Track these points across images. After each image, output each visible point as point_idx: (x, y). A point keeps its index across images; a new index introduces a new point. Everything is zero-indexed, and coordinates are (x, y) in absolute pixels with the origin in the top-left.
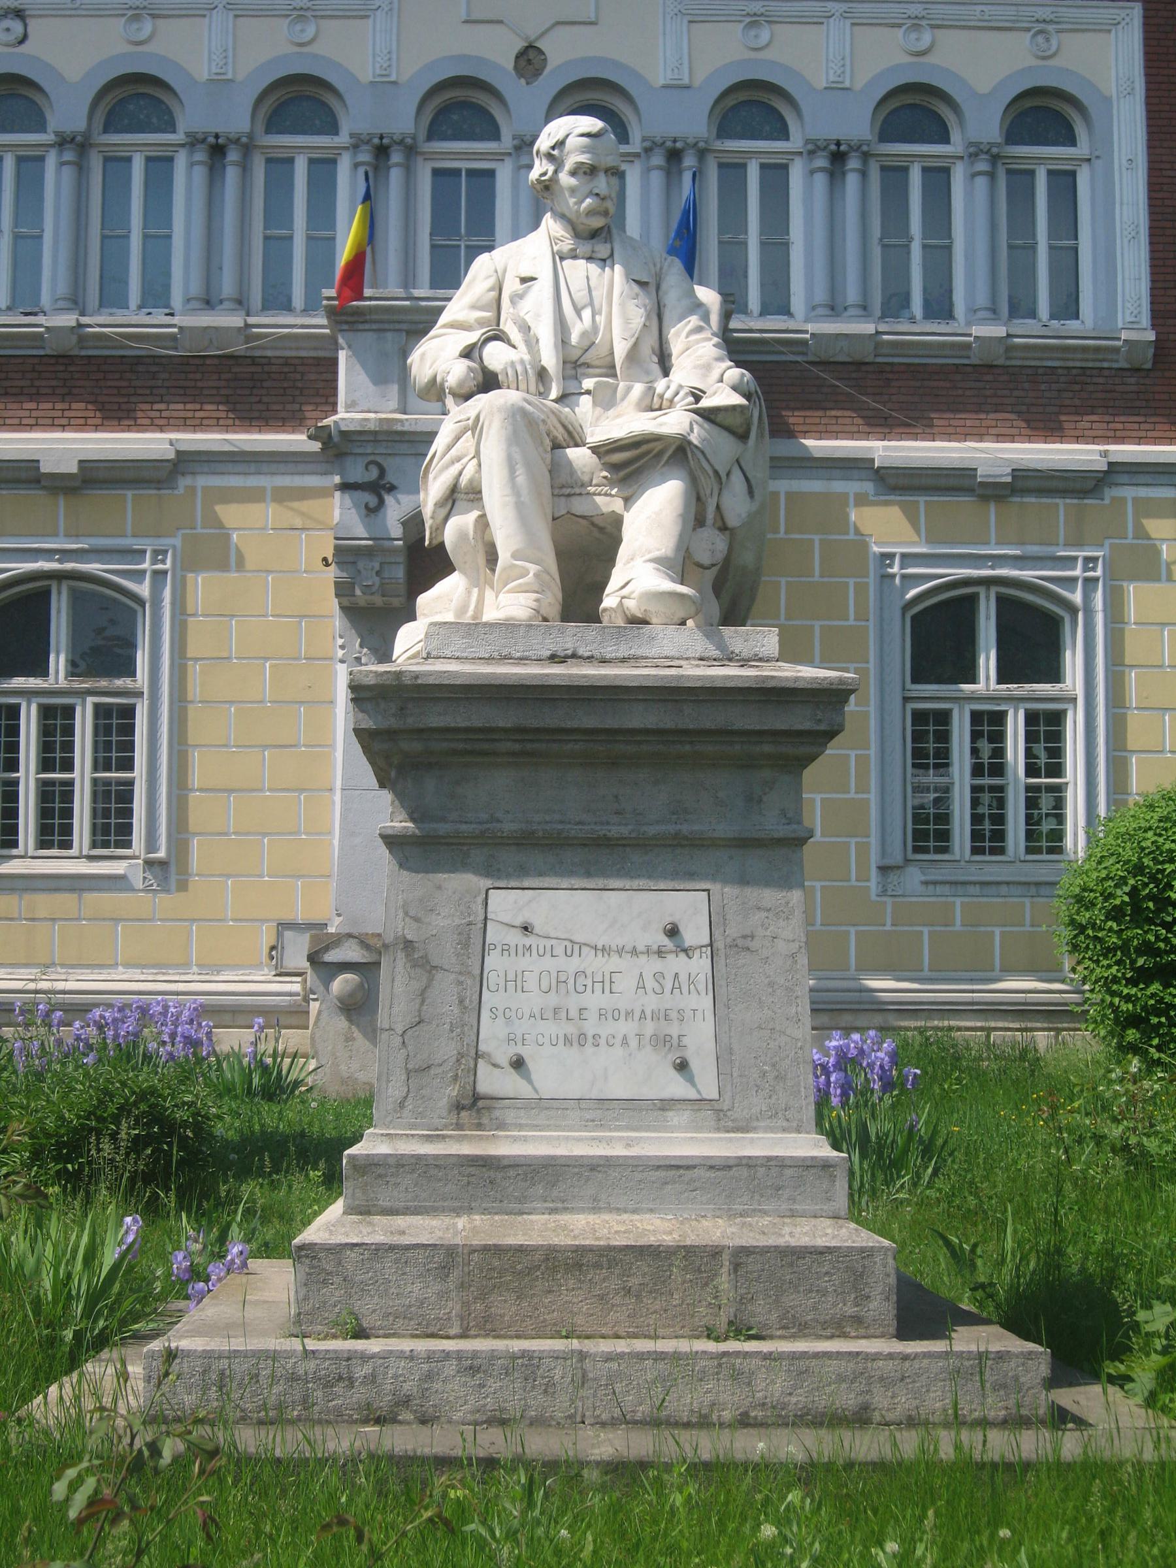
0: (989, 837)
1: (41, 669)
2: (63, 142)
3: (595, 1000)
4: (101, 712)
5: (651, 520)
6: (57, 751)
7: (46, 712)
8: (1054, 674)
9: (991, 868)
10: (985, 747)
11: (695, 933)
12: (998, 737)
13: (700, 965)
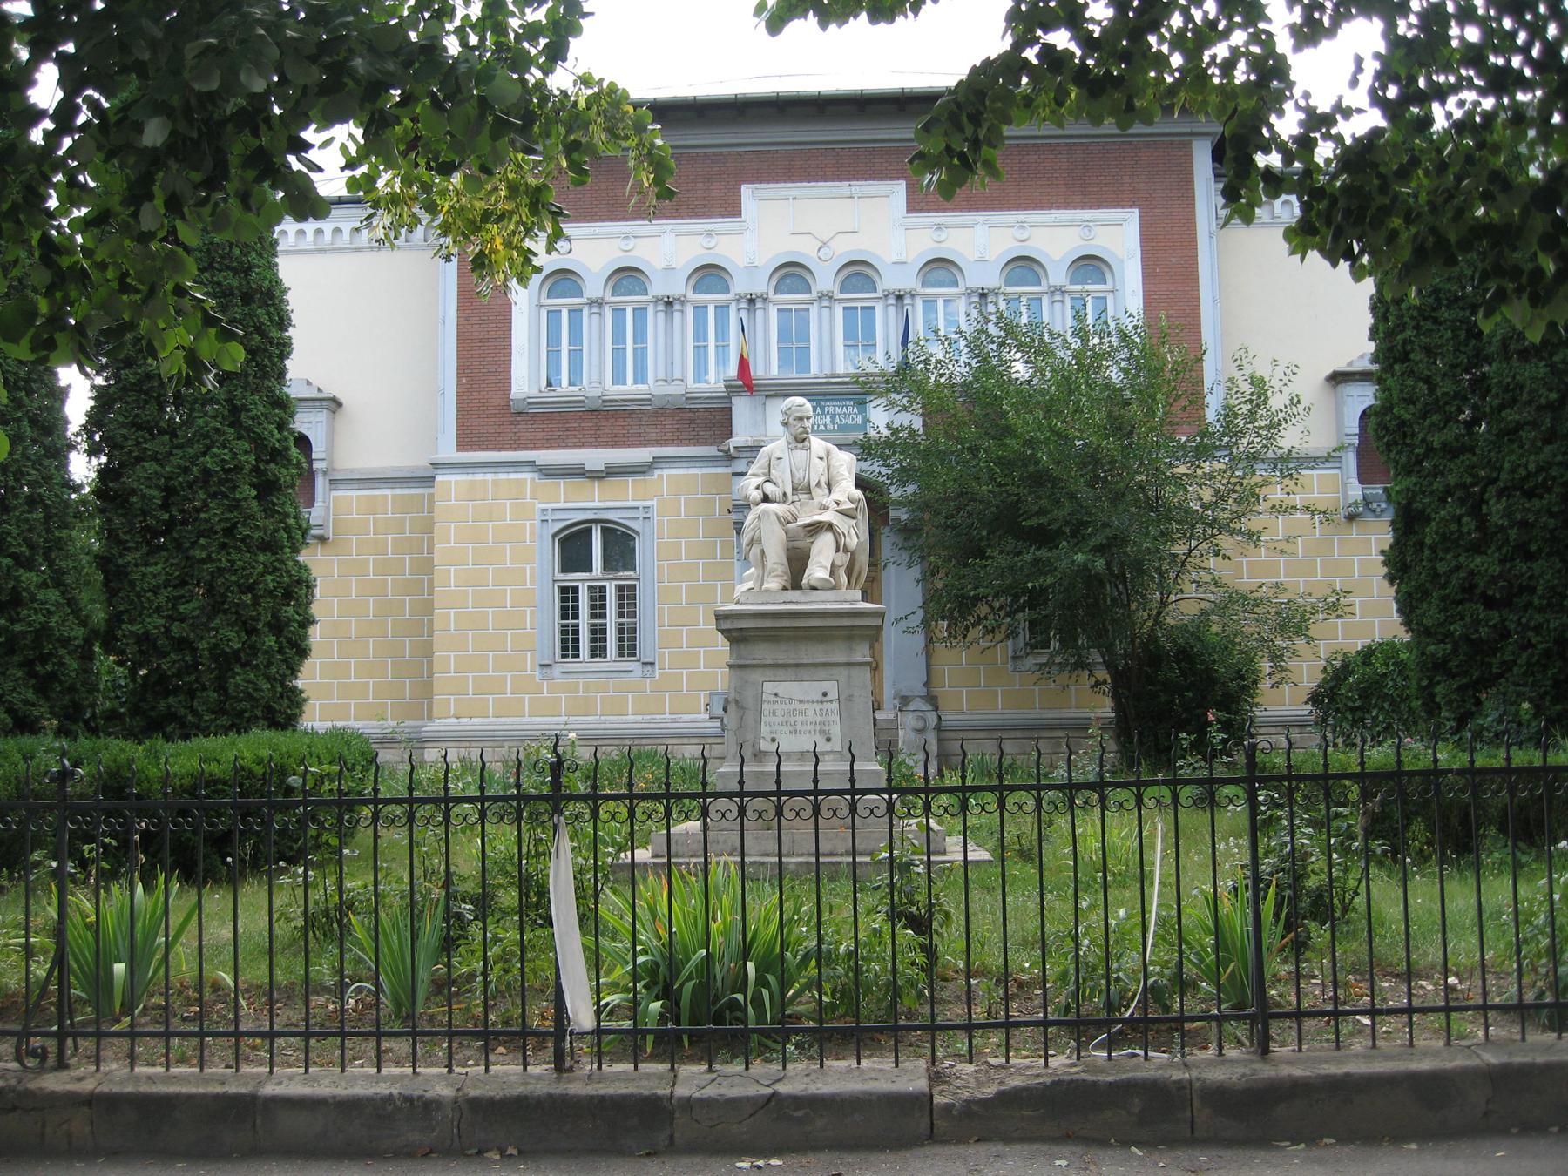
2: (592, 303)
3: (800, 718)
4: (620, 588)
6: (598, 610)
11: (833, 695)
13: (835, 706)
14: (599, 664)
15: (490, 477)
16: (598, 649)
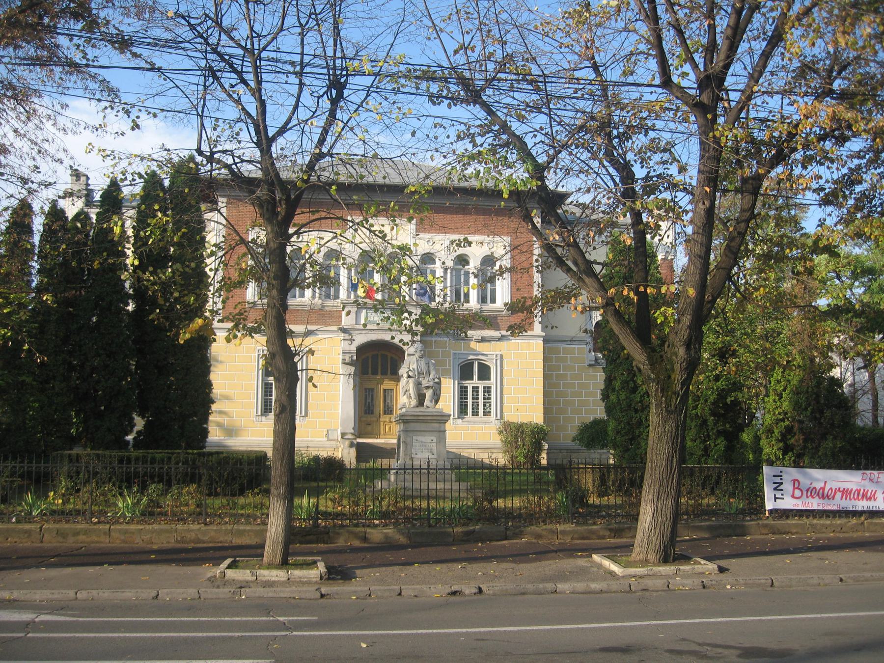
0: (475, 413)
5: (429, 394)
9: (475, 418)
10: (475, 394)
12: (478, 392)
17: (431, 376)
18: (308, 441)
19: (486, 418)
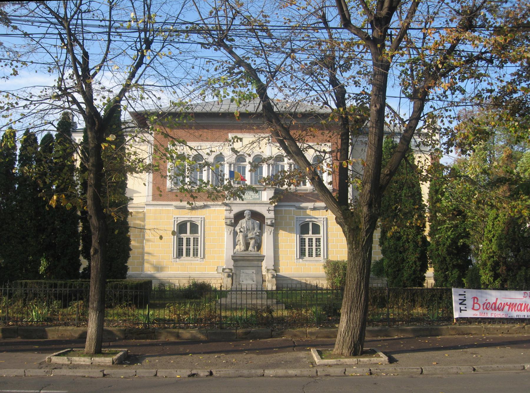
0: (310, 255)
1: (186, 233)
5: (252, 242)
6: (188, 244)
7: (187, 239)
8: (320, 234)
9: (311, 258)
12: (312, 241)
14: (188, 258)
15: (161, 208)
16: (188, 254)
17: (255, 232)
18: (205, 274)
19: (317, 258)
